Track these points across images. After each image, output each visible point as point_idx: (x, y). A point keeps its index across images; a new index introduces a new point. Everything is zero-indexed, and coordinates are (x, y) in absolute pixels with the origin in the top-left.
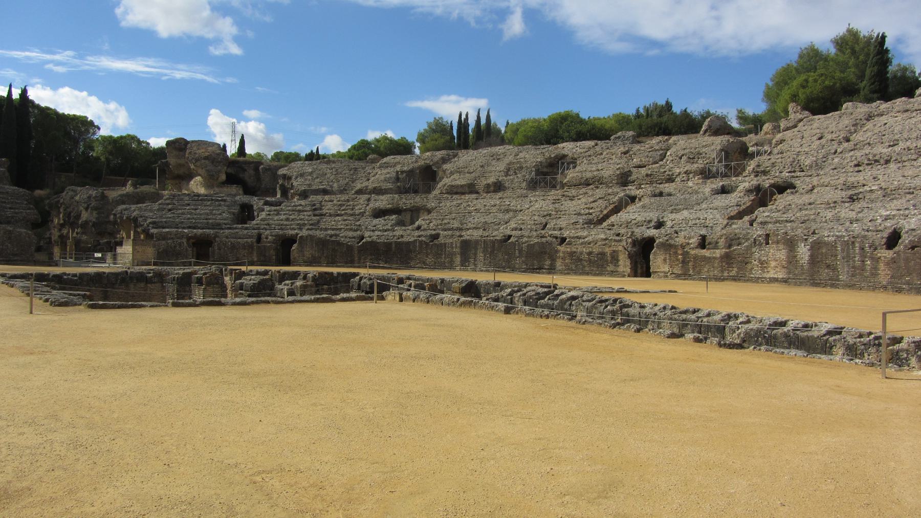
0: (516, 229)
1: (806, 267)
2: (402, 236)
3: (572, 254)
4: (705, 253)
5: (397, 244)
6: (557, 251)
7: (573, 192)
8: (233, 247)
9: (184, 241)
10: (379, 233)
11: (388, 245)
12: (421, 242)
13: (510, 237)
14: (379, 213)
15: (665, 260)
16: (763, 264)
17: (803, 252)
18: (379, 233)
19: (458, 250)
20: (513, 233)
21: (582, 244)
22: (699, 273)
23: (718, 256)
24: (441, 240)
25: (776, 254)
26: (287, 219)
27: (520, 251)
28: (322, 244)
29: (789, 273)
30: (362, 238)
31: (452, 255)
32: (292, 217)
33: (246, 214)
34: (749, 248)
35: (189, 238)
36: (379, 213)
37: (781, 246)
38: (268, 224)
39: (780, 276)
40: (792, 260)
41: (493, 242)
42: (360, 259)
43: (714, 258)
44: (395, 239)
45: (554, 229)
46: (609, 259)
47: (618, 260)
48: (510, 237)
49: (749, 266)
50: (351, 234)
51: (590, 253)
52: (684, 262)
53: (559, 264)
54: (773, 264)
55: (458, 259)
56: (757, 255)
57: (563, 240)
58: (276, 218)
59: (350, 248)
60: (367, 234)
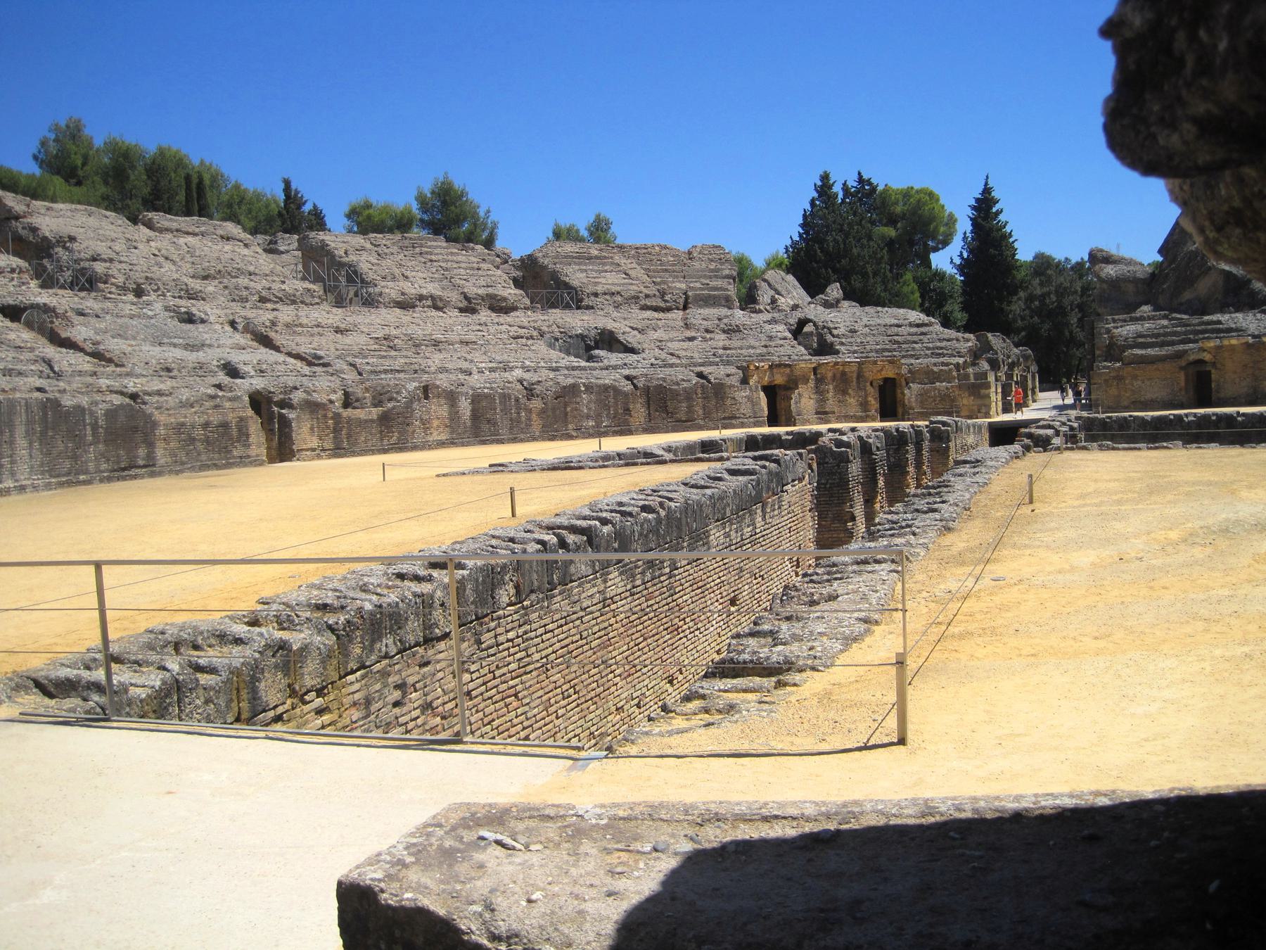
1: (469, 423)
4: (360, 414)
15: (312, 429)
16: (426, 425)
17: (465, 406)
22: (355, 443)
23: (375, 417)
25: (439, 409)
29: (451, 433)
34: (409, 405)
37: (443, 401)
39: (443, 437)
40: (454, 416)
43: (372, 421)
47: (248, 436)
49: (410, 429)
51: (206, 425)
52: (336, 431)
54: (435, 423)
56: (417, 414)
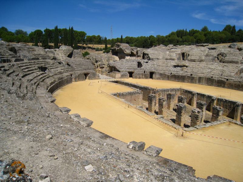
0: (213, 75)
2: (182, 74)
3: (230, 84)
5: (181, 76)
6: (226, 83)
7: (226, 64)
8: (139, 74)
9: (127, 72)
10: (176, 72)
11: (178, 76)
12: (187, 76)
13: (212, 77)
14: (175, 66)
18: (176, 72)
19: (198, 79)
20: (213, 76)
21: (233, 81)
24: (193, 76)
26: (151, 67)
27: (215, 81)
28: (161, 74)
30: (171, 73)
31: (196, 80)
32: (152, 66)
33: (140, 65)
35: (128, 72)
36: (175, 66)
38: (146, 68)
41: (208, 78)
42: (171, 78)
44: (180, 74)
45: (224, 76)
46: (241, 86)
48: (212, 77)
50: (168, 72)
51: (235, 84)
53: (226, 86)
55: (197, 81)
57: (227, 80)
58: (148, 66)
59: (168, 76)
60: (172, 72)
